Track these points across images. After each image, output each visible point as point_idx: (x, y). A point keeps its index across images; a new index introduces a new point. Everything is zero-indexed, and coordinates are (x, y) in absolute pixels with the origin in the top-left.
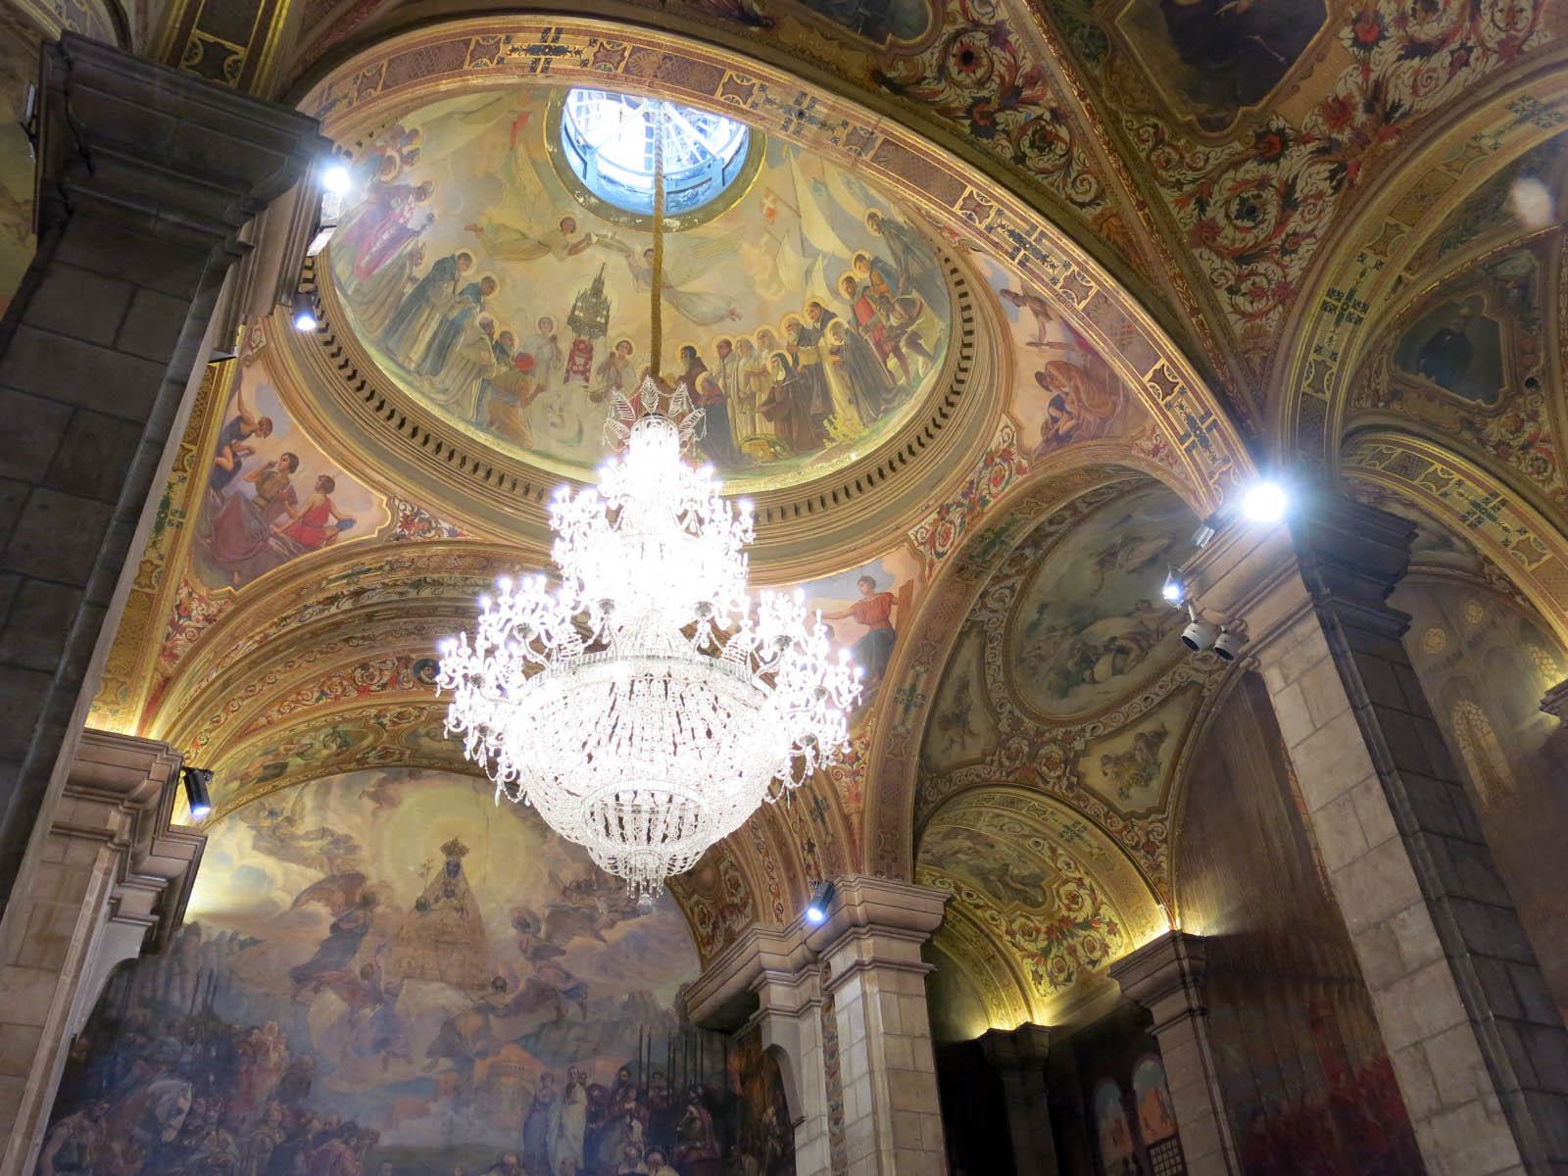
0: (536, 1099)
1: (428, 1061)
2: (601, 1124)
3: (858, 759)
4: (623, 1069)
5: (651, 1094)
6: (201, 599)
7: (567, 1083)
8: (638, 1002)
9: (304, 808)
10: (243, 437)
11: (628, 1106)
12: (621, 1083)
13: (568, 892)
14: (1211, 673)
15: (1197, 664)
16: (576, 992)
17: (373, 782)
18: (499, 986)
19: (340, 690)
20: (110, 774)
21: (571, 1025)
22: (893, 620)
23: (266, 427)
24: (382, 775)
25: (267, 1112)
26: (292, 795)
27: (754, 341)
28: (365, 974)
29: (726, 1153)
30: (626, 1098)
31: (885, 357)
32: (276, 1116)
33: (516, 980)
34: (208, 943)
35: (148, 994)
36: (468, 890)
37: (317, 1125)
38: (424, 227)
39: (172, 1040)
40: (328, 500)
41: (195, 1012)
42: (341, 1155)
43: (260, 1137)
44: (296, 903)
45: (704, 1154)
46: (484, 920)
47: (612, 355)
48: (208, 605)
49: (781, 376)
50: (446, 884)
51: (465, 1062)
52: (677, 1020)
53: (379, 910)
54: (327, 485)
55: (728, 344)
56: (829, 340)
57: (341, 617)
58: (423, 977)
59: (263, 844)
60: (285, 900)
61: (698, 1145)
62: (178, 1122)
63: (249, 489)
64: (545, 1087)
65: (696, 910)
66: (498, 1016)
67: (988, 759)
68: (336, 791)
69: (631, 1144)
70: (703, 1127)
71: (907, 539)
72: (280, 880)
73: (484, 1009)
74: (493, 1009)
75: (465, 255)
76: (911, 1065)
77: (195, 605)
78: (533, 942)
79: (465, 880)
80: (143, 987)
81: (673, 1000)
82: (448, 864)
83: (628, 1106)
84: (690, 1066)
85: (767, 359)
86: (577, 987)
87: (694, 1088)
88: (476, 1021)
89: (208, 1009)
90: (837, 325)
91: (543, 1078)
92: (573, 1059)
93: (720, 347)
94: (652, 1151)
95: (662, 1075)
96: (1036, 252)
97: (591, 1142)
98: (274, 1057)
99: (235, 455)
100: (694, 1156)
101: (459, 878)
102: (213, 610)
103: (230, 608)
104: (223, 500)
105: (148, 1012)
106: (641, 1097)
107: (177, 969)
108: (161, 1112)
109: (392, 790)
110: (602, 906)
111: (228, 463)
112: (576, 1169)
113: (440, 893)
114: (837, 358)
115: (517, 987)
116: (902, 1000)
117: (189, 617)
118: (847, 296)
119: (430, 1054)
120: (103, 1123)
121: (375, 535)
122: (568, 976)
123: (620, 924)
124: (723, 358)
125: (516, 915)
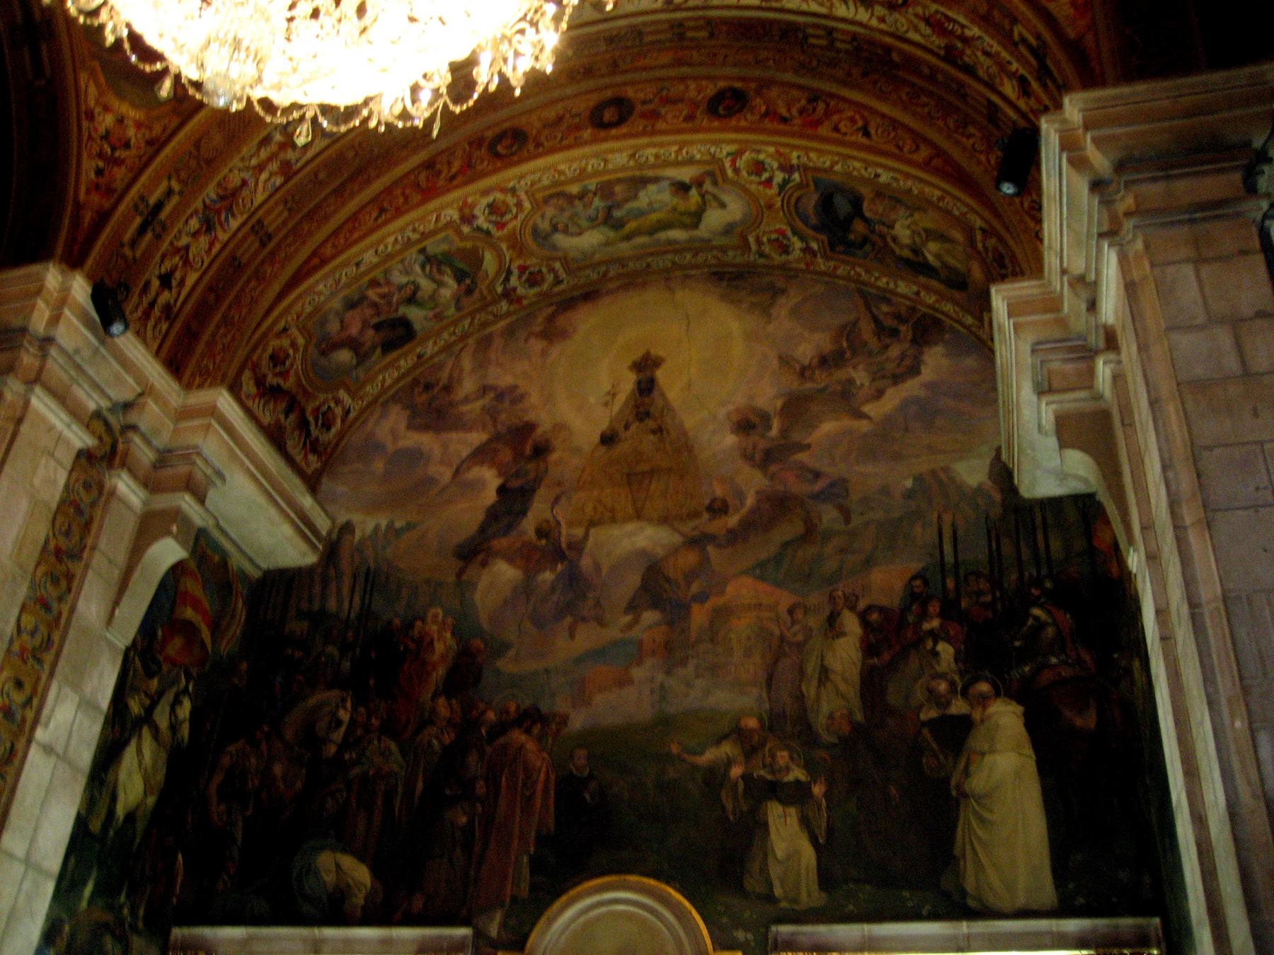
0: (782, 638)
1: (628, 619)
2: (886, 656)
4: (914, 578)
5: (964, 604)
6: (139, 125)
7: (827, 612)
8: (934, 487)
9: (462, 371)
11: (927, 626)
13: (807, 374)
17: (540, 320)
18: (718, 508)
19: (401, 200)
21: (828, 536)
25: (433, 711)
28: (541, 533)
30: (924, 615)
33: (741, 496)
34: (362, 542)
35: (304, 606)
36: (667, 406)
37: (491, 716)
41: (353, 615)
42: (522, 747)
44: (457, 472)
45: (1066, 673)
46: (691, 434)
50: (637, 406)
51: (675, 612)
52: (997, 497)
53: (554, 457)
58: (613, 520)
61: (1054, 660)
62: (338, 736)
64: (794, 623)
66: (719, 546)
73: (697, 542)
76: (1231, 363)
78: (762, 445)
79: (663, 395)
81: (986, 469)
82: (639, 383)
83: (927, 626)
84: (1026, 553)
87: (1038, 582)
91: (791, 612)
94: (976, 679)
95: (978, 575)
97: (872, 684)
98: (439, 647)
100: (1046, 677)
101: (656, 393)
105: (305, 624)
106: (950, 610)
107: (332, 573)
108: (321, 726)
110: (861, 376)
113: (631, 418)
115: (742, 504)
116: (1205, 271)
119: (633, 608)
120: (264, 747)
122: (817, 475)
123: (890, 392)
125: (735, 418)
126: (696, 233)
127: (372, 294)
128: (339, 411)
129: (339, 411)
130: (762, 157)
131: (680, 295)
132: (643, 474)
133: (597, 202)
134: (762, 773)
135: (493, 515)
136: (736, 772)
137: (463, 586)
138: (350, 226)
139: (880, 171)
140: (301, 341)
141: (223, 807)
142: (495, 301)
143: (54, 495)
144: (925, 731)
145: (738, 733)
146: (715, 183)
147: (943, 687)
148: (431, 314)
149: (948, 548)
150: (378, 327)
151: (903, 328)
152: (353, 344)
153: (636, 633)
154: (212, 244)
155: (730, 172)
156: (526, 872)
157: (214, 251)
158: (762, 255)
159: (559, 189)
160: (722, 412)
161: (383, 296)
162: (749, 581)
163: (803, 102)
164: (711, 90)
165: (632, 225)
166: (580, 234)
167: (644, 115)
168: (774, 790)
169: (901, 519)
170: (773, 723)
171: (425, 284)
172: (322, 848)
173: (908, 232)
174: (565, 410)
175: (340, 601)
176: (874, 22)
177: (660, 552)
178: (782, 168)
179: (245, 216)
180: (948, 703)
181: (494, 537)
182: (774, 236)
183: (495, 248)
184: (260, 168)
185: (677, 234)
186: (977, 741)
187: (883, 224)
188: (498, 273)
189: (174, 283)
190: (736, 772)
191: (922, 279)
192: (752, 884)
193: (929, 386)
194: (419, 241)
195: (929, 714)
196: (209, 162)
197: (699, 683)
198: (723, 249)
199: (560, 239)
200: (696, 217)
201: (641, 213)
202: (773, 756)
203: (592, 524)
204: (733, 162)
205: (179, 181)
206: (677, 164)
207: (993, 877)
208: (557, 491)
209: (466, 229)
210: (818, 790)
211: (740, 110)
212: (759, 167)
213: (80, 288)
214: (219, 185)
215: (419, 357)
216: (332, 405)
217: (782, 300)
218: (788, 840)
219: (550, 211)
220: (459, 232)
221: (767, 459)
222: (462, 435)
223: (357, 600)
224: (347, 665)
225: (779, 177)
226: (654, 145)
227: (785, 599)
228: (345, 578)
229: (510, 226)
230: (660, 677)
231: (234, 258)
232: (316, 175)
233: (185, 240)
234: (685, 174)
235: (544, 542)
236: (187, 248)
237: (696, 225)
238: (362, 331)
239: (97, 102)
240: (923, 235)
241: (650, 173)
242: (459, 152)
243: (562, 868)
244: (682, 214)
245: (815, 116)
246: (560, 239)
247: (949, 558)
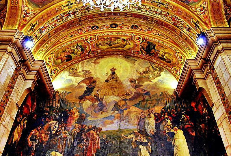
2: (159, 121)
3: (204, 8)
4: (163, 109)
6: (32, 10)
9: (79, 67)
11: (165, 117)
12: (162, 112)
16: (148, 93)
19: (75, 34)
20: (6, 38)
21: (147, 101)
24: (95, 59)
26: (76, 65)
30: (165, 115)
32: (77, 126)
33: (132, 93)
34: (60, 94)
37: (87, 128)
42: (93, 134)
43: (74, 131)
48: (34, 12)
52: (175, 97)
53: (97, 83)
57: (72, 19)
58: (109, 95)
59: (71, 75)
60: (77, 84)
61: (187, 124)
62: (55, 129)
64: (142, 115)
65: (174, 71)
68: (86, 63)
69: (168, 125)
70: (187, 119)
72: (75, 80)
74: (127, 99)
78: (135, 84)
80: (47, 104)
82: (112, 72)
83: (165, 117)
86: (147, 92)
88: (123, 102)
94: (175, 126)
97: (157, 126)
98: (76, 115)
100: (186, 126)
102: (35, 12)
103: (39, 11)
106: (169, 114)
108: (52, 128)
109: (97, 61)
117: (29, 14)
122: (145, 91)
123: (156, 78)
125: (130, 80)
126: (124, 49)
127: (67, 50)
128: (57, 71)
129: (57, 71)
130: (140, 37)
131: (118, 59)
132: (114, 87)
133: (109, 41)
134: (139, 140)
137: (80, 104)
138: (65, 37)
139: (161, 41)
140: (54, 56)
141: (31, 142)
142: (86, 56)
143: (11, 75)
144: (167, 134)
145: (134, 133)
146: (130, 40)
147: (169, 127)
148: (75, 56)
150: (66, 57)
151: (157, 68)
152: (61, 59)
153: (113, 115)
154: (41, 36)
155: (133, 39)
157: (41, 37)
158: (133, 54)
159: (103, 37)
160: (127, 79)
161: (69, 51)
162: (134, 107)
163: (147, 29)
164: (131, 25)
165: (113, 46)
166: (104, 46)
167: (120, 27)
168: (141, 143)
169: (159, 99)
170: (141, 132)
171: (76, 50)
173: (162, 52)
174: (98, 75)
175: (56, 105)
176: (161, 18)
177: (118, 101)
178: (142, 39)
179: (47, 32)
180: (170, 130)
182: (137, 51)
183: (89, 46)
184: (51, 24)
185: (120, 48)
187: (158, 50)
188: (88, 51)
189: (34, 41)
190: (134, 140)
191: (162, 61)
194: (77, 42)
195: (167, 131)
196: (44, 20)
197: (126, 124)
198: (127, 52)
199: (100, 46)
200: (125, 46)
201: (116, 44)
202: (141, 138)
203: (105, 95)
204: (134, 37)
205: (38, 22)
206: (124, 36)
208: (98, 89)
209: (85, 41)
210: (149, 144)
211: (137, 28)
212: (139, 38)
214: (44, 25)
215: (72, 63)
216: (56, 69)
217: (136, 62)
219: (100, 41)
220: (84, 42)
221: (136, 87)
222: (79, 78)
223: (59, 105)
224: (57, 116)
225: (142, 40)
226: (121, 32)
227: (140, 110)
228: (57, 101)
229: (93, 42)
230: (119, 122)
231: (44, 39)
232: (60, 28)
233: (37, 34)
234: (125, 38)
235: (96, 97)
236: (37, 35)
237: (124, 48)
238: (63, 57)
239: (25, 4)
240: (165, 53)
241: (119, 37)
242: (86, 28)
244: (122, 45)
245: (150, 31)
246: (100, 46)
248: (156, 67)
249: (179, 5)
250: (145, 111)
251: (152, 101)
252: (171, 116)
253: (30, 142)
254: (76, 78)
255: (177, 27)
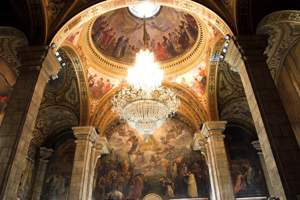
2: (179, 168)
5: (188, 162)
6: (95, 103)
8: (184, 148)
10: (93, 78)
12: (182, 161)
14: (276, 65)
15: (272, 64)
16: (173, 148)
18: (160, 149)
21: (172, 153)
22: (205, 74)
23: (96, 76)
25: (127, 173)
27: (174, 31)
28: (138, 151)
29: (202, 170)
30: (183, 164)
31: (194, 26)
33: (162, 148)
34: (115, 151)
35: (108, 159)
38: (114, 35)
39: (113, 165)
40: (109, 83)
42: (139, 178)
47: (152, 42)
49: (180, 36)
53: (139, 141)
54: (108, 81)
55: (170, 33)
56: (186, 27)
58: (147, 150)
59: (120, 135)
63: (97, 85)
67: (234, 94)
70: (198, 166)
71: (204, 59)
75: (123, 36)
76: (220, 152)
77: (94, 104)
80: (108, 158)
84: (194, 157)
85: (177, 34)
86: (173, 147)
87: (195, 160)
89: (117, 160)
90: (186, 23)
91: (169, 163)
92: (173, 159)
93: (169, 34)
94: (189, 171)
96: (190, 6)
97: (178, 171)
98: (127, 165)
99: (92, 81)
100: (196, 171)
102: (97, 104)
104: (93, 88)
105: (109, 162)
106: (186, 163)
108: (113, 175)
110: (175, 133)
111: (91, 83)
112: (176, 176)
114: (187, 29)
116: (218, 142)
117: (94, 106)
118: (185, 18)
119: (150, 161)
121: (118, 86)
122: (171, 146)
123: (179, 136)
124: (170, 36)
135: (132, 148)
136: (164, 181)
141: (101, 185)
145: (164, 177)
147: (186, 172)
149: (186, 156)
152: (114, 126)
153: (151, 165)
156: (141, 193)
169: (180, 152)
172: (115, 191)
175: (113, 159)
181: (132, 151)
186: (189, 178)
190: (164, 181)
192: (166, 194)
193: (183, 135)
195: (184, 175)
203: (145, 150)
207: (192, 194)
210: (173, 184)
213: (94, 129)
218: (170, 189)
221: (165, 143)
224: (115, 167)
230: (154, 170)
243: (145, 193)
247: (186, 157)
248: (179, 126)
249: (191, 95)
250: (171, 161)
251: (175, 153)
252: (187, 164)
253: (101, 186)
254: (124, 137)
255: (191, 104)
